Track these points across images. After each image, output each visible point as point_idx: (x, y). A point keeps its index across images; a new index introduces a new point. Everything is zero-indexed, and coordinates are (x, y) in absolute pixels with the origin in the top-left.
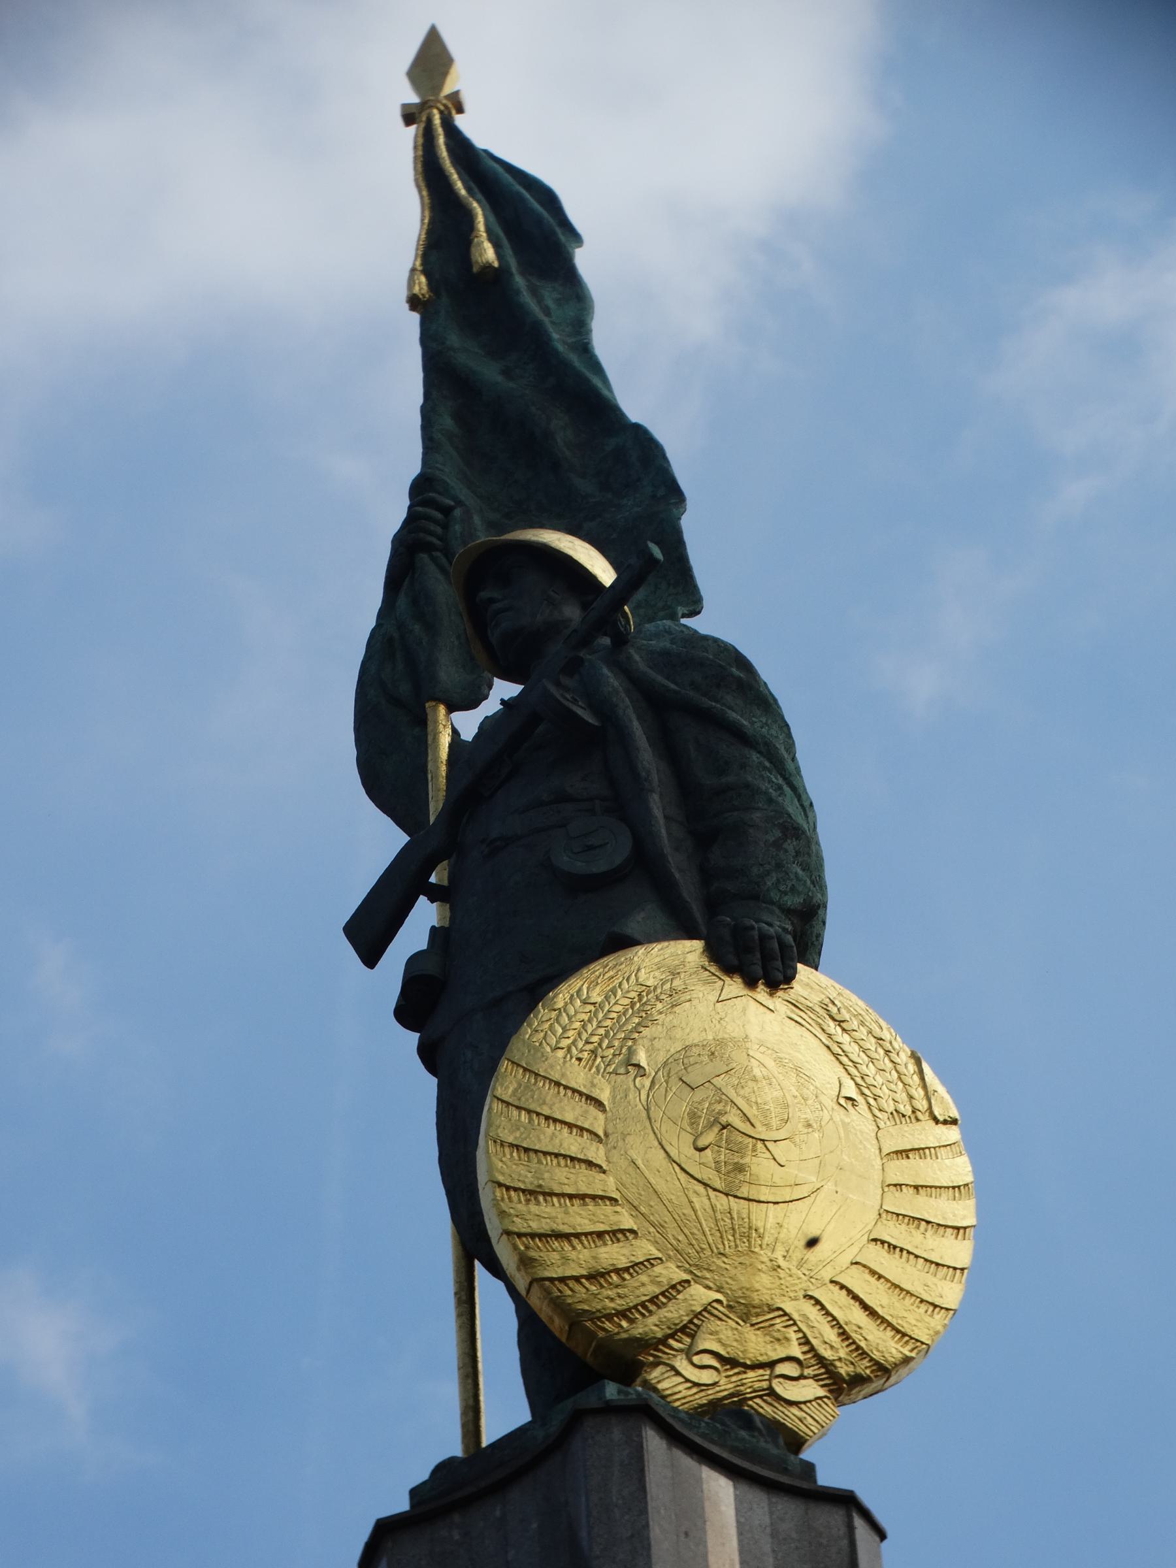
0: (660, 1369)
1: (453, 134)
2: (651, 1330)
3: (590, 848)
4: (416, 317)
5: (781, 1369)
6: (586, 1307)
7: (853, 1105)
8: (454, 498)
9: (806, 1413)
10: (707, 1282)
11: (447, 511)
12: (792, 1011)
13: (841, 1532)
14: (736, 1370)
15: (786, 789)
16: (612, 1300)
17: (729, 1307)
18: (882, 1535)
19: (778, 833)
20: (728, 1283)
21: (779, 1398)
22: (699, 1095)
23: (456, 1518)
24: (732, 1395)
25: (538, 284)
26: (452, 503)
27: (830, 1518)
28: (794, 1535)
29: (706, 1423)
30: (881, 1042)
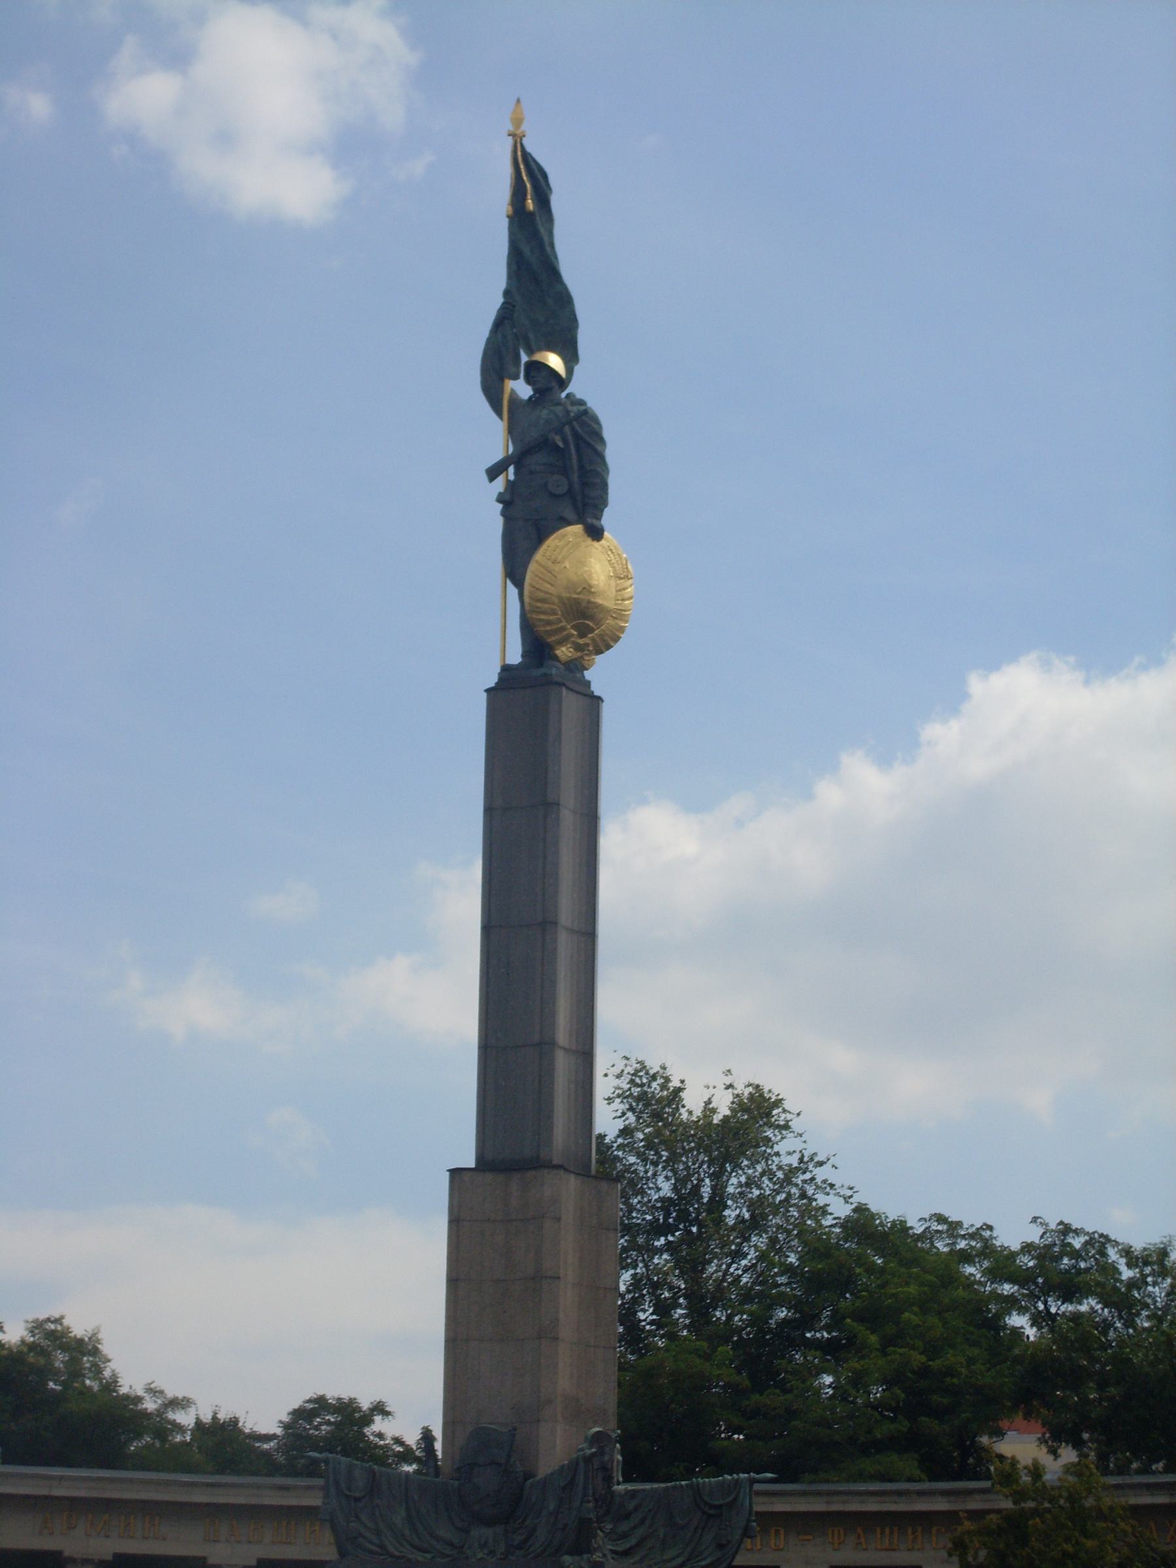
1: (522, 145)
5: (586, 652)
11: (514, 306)
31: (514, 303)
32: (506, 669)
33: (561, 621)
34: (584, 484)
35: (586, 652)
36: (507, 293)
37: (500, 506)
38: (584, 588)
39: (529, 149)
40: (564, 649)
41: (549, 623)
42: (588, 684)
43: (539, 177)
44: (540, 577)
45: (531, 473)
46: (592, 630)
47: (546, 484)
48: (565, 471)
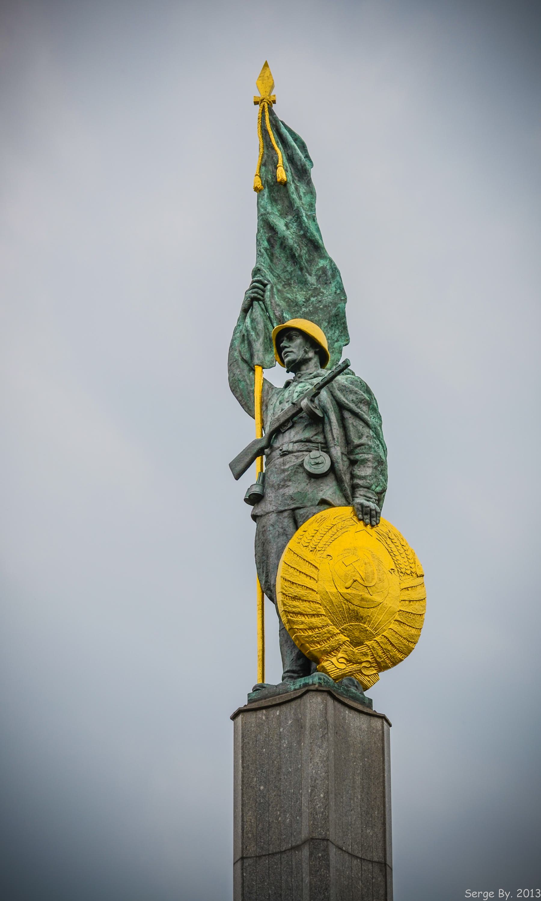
0: (329, 662)
1: (271, 113)
2: (327, 649)
3: (318, 464)
4: (256, 194)
5: (364, 664)
6: (308, 640)
7: (394, 572)
8: (269, 281)
9: (370, 679)
10: (345, 634)
12: (378, 536)
13: (380, 728)
14: (351, 664)
15: (380, 445)
16: (316, 638)
17: (350, 643)
18: (390, 725)
19: (376, 464)
20: (351, 635)
21: (362, 673)
22: (349, 568)
23: (264, 711)
24: (349, 672)
25: (298, 185)
26: (267, 283)
27: (377, 723)
28: (366, 729)
29: (343, 688)
30: (403, 547)
31: (266, 282)
32: (255, 689)
33: (328, 625)
34: (353, 463)
35: (364, 664)
36: (257, 271)
37: (250, 508)
38: (355, 581)
39: (280, 115)
40: (334, 660)
41: (311, 628)
42: (369, 703)
43: (293, 144)
44: (295, 569)
45: (284, 454)
46: (371, 637)
47: (301, 465)
48: (326, 448)
